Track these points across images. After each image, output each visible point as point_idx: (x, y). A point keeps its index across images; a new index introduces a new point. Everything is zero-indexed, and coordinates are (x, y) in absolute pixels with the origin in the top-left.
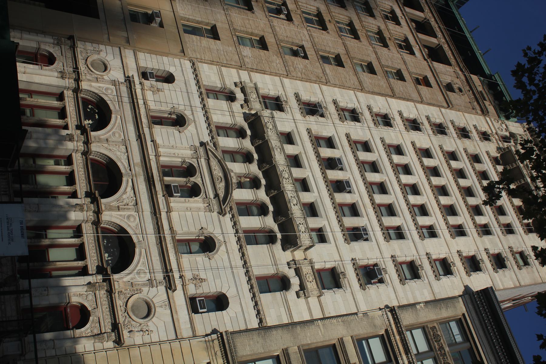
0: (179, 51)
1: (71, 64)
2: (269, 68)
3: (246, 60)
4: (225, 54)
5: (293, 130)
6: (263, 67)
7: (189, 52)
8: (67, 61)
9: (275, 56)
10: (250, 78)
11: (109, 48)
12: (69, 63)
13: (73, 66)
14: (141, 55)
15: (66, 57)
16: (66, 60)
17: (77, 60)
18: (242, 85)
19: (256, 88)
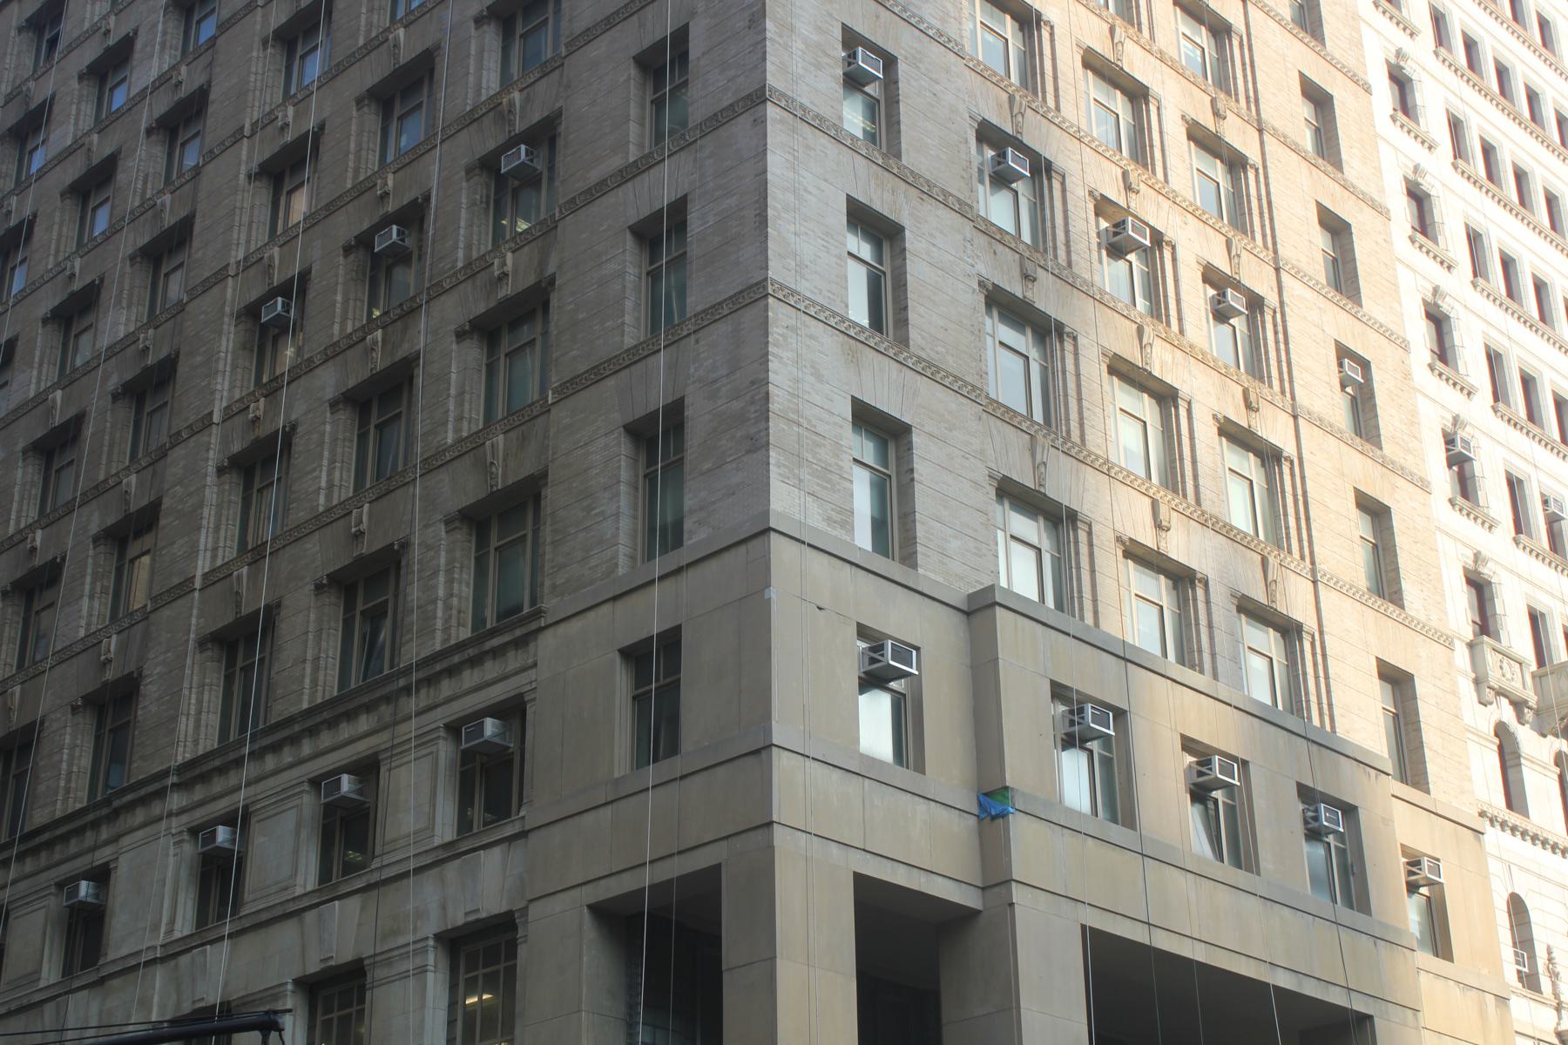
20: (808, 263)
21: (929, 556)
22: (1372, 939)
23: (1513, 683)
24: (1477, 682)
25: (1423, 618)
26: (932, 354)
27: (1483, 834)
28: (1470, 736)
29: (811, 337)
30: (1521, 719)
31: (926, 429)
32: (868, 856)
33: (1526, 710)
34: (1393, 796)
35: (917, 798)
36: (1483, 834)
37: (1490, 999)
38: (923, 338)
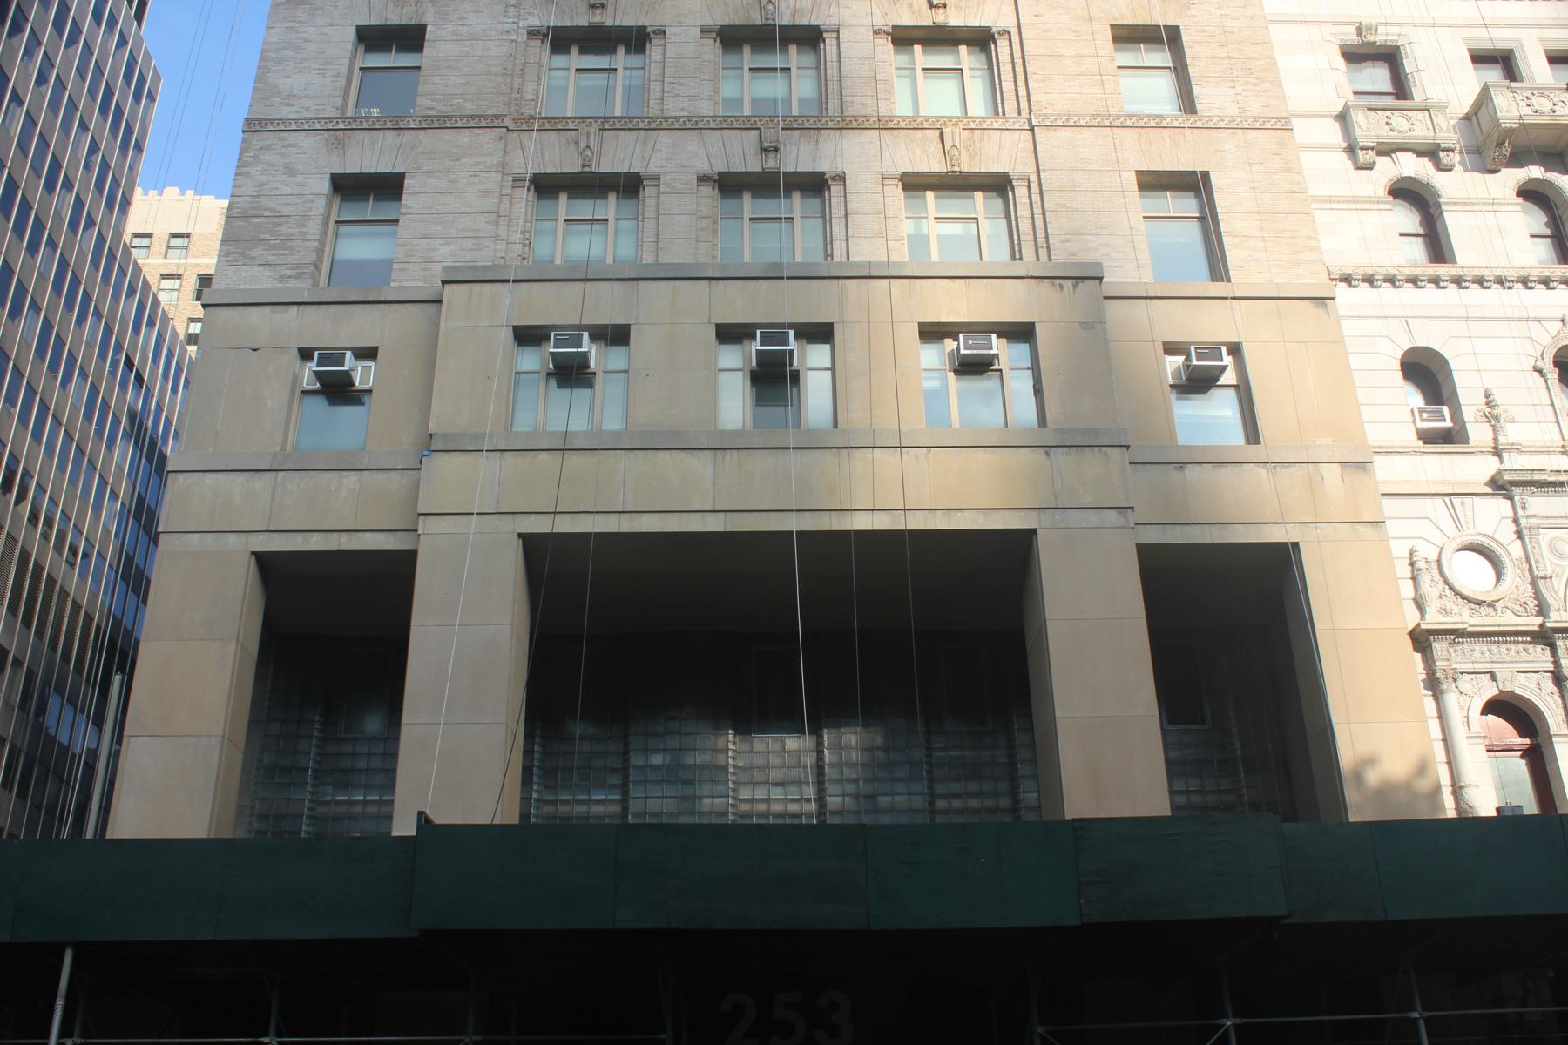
0: (1321, 312)
1: (1513, 646)
2: (1257, 44)
3: (1255, 108)
4: (1261, 168)
5: (1464, 39)
6: (1261, 62)
7: (1316, 283)
8: (1508, 659)
9: (1189, 13)
10: (1313, 116)
11: (1392, 528)
12: (1513, 653)
13: (1522, 642)
14: (1376, 435)
15: (1492, 662)
16: (1505, 662)
17: (1510, 628)
18: (1372, 149)
19: (1369, 109)
20: (295, 92)
21: (408, 269)
22: (1042, 450)
23: (1415, 133)
24: (1351, 150)
25: (1232, 110)
26: (444, 109)
27: (1333, 299)
28: (1314, 206)
29: (290, 146)
30: (1440, 167)
31: (425, 169)
32: (274, 535)
33: (1442, 155)
34: (1105, 298)
35: (345, 473)
36: (1333, 299)
37: (1332, 473)
38: (435, 100)
